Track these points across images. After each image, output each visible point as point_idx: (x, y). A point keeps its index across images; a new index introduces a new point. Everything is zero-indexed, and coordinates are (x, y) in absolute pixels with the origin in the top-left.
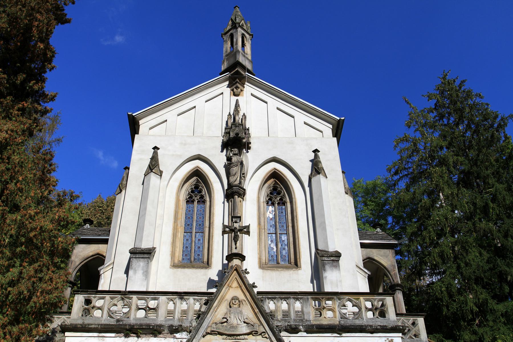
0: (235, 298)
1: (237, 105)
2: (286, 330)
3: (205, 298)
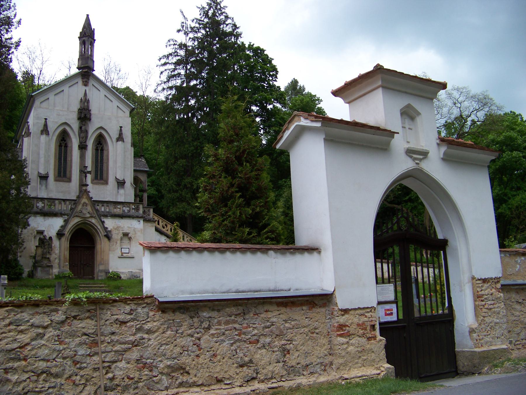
0: (85, 203)
1: (85, 94)
2: (103, 216)
3: (73, 202)
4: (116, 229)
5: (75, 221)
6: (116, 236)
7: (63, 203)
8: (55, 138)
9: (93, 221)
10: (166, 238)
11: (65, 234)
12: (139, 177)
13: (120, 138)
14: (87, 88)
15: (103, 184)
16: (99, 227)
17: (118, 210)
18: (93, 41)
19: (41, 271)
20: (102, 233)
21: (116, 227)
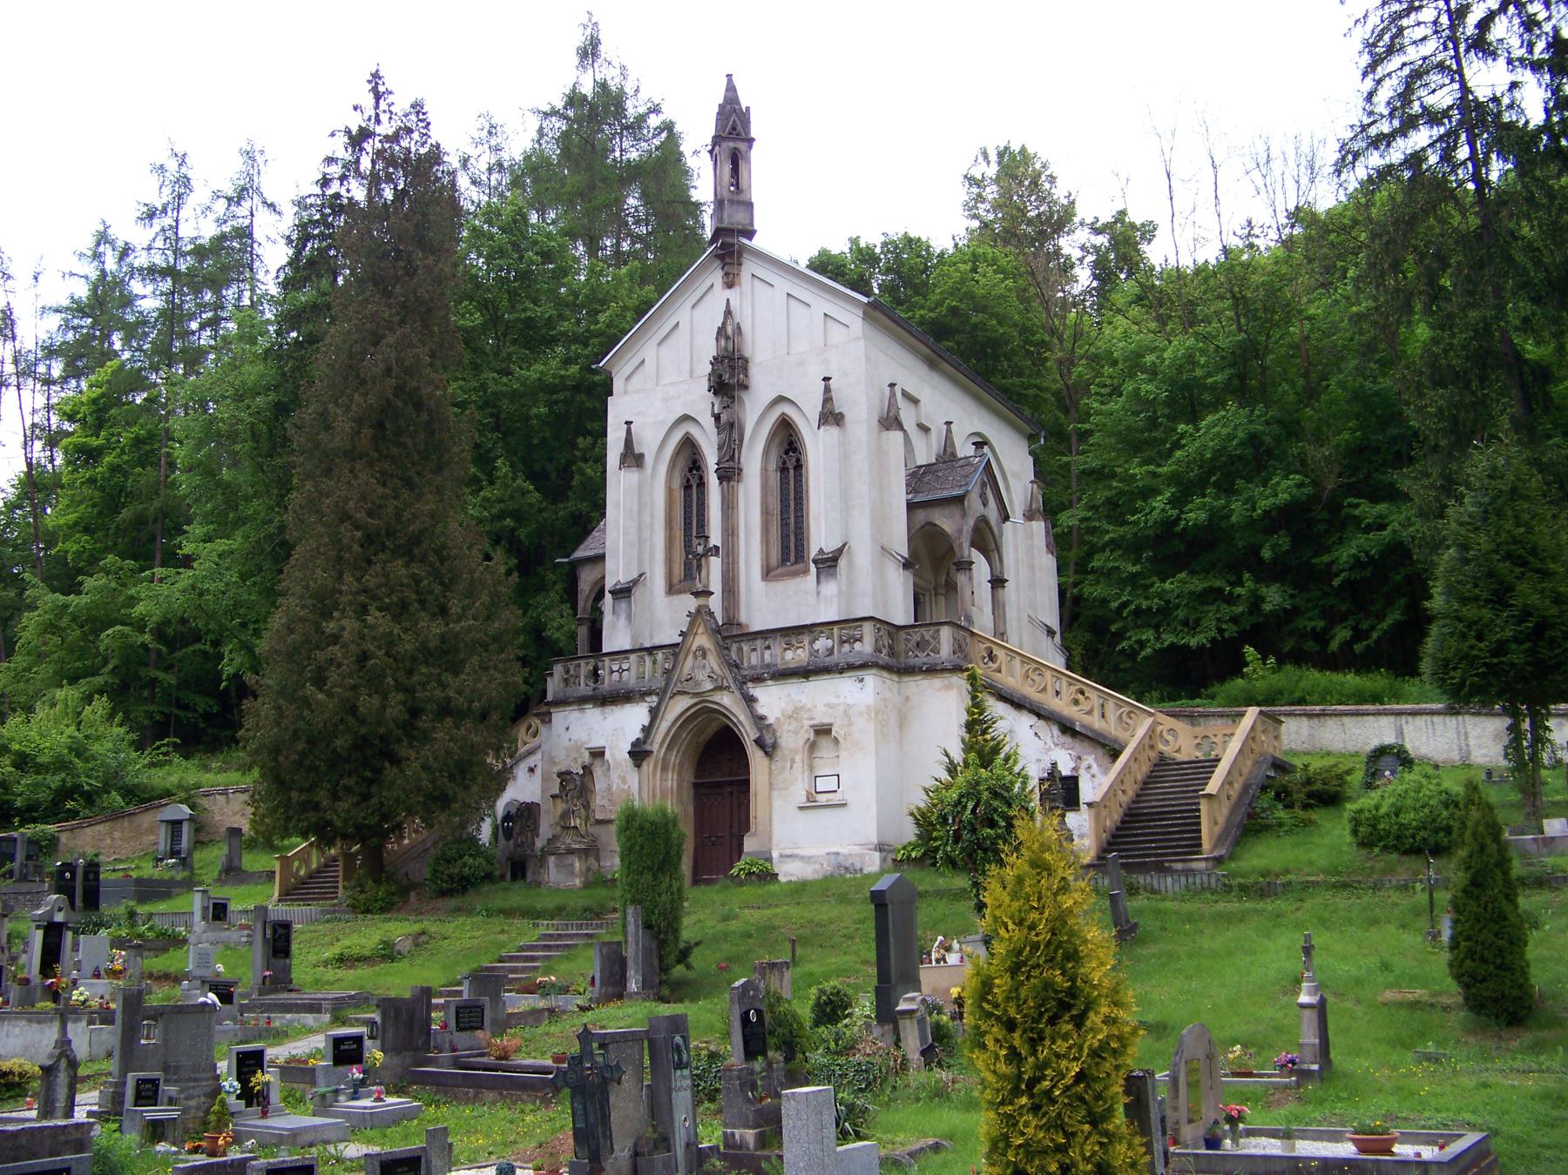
1: (728, 313)
4: (790, 717)
5: (679, 706)
6: (792, 740)
7: (648, 659)
8: (663, 469)
9: (727, 700)
10: (1033, 720)
11: (652, 752)
12: (937, 522)
13: (831, 416)
14: (732, 294)
15: (795, 574)
16: (742, 718)
17: (797, 656)
18: (742, 146)
19: (557, 866)
20: (749, 734)
21: (790, 709)
